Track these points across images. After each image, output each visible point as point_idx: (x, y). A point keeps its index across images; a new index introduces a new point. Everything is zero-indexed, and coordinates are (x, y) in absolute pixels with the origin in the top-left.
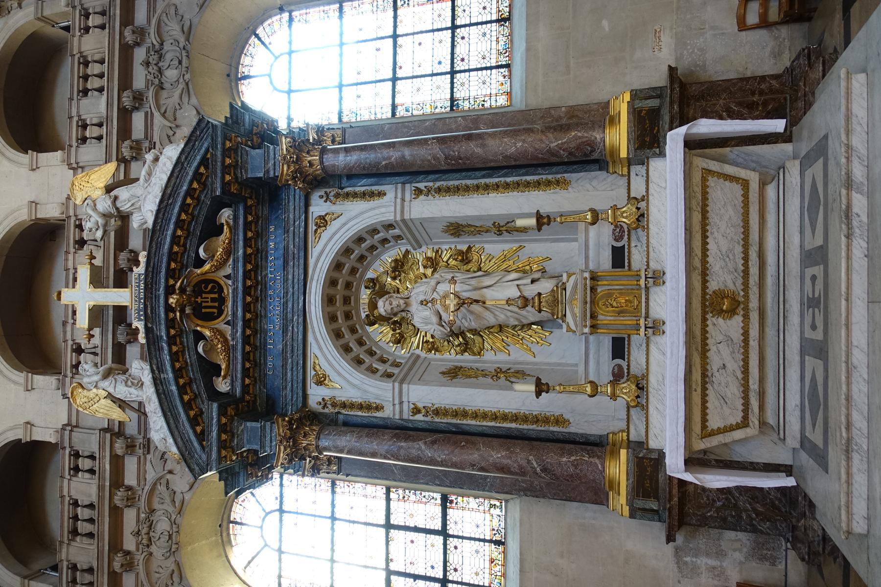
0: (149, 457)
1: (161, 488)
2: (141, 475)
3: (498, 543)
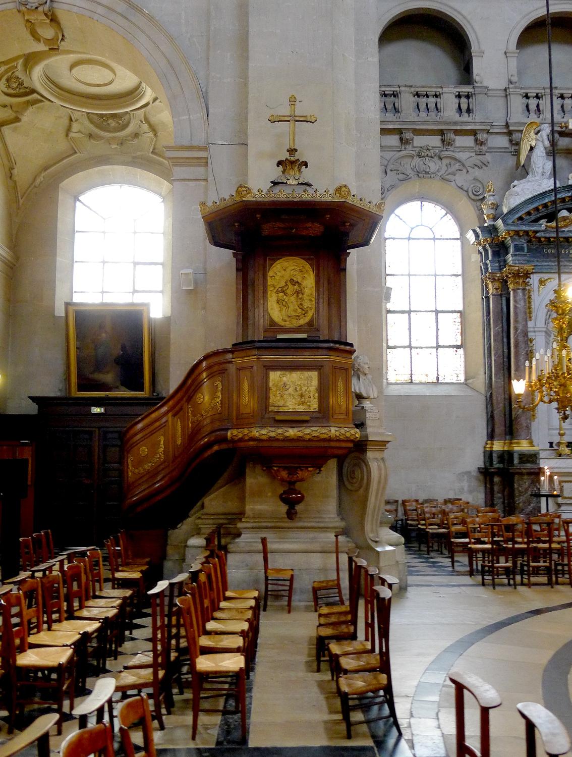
0: (473, 154)
1: (457, 166)
2: (464, 149)
3: (438, 379)
